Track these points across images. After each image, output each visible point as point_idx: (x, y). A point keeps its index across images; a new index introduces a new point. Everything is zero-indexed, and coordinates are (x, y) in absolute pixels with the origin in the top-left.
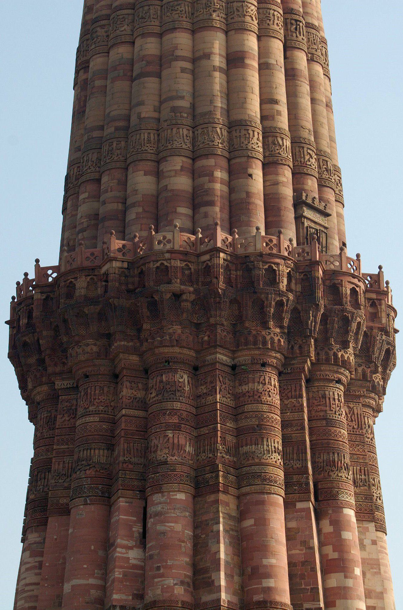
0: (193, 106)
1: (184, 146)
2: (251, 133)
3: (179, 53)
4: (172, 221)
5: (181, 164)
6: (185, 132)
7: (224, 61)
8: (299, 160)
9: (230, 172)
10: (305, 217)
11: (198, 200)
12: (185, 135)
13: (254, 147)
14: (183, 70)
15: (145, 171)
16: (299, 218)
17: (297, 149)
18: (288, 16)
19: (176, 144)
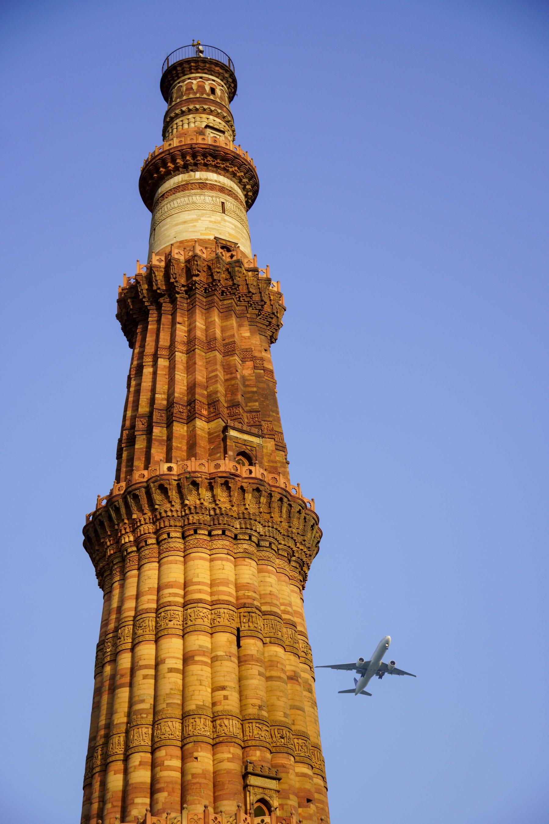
0: (155, 706)
1: (142, 743)
2: (197, 720)
3: (141, 663)
4: (130, 811)
5: (140, 760)
6: (144, 730)
7: (181, 662)
8: (248, 735)
9: (183, 759)
10: (251, 786)
11: (153, 789)
12: (143, 733)
13: (200, 732)
14: (145, 677)
15: (115, 771)
16: (246, 787)
17: (247, 725)
18: (242, 610)
19: (136, 743)
